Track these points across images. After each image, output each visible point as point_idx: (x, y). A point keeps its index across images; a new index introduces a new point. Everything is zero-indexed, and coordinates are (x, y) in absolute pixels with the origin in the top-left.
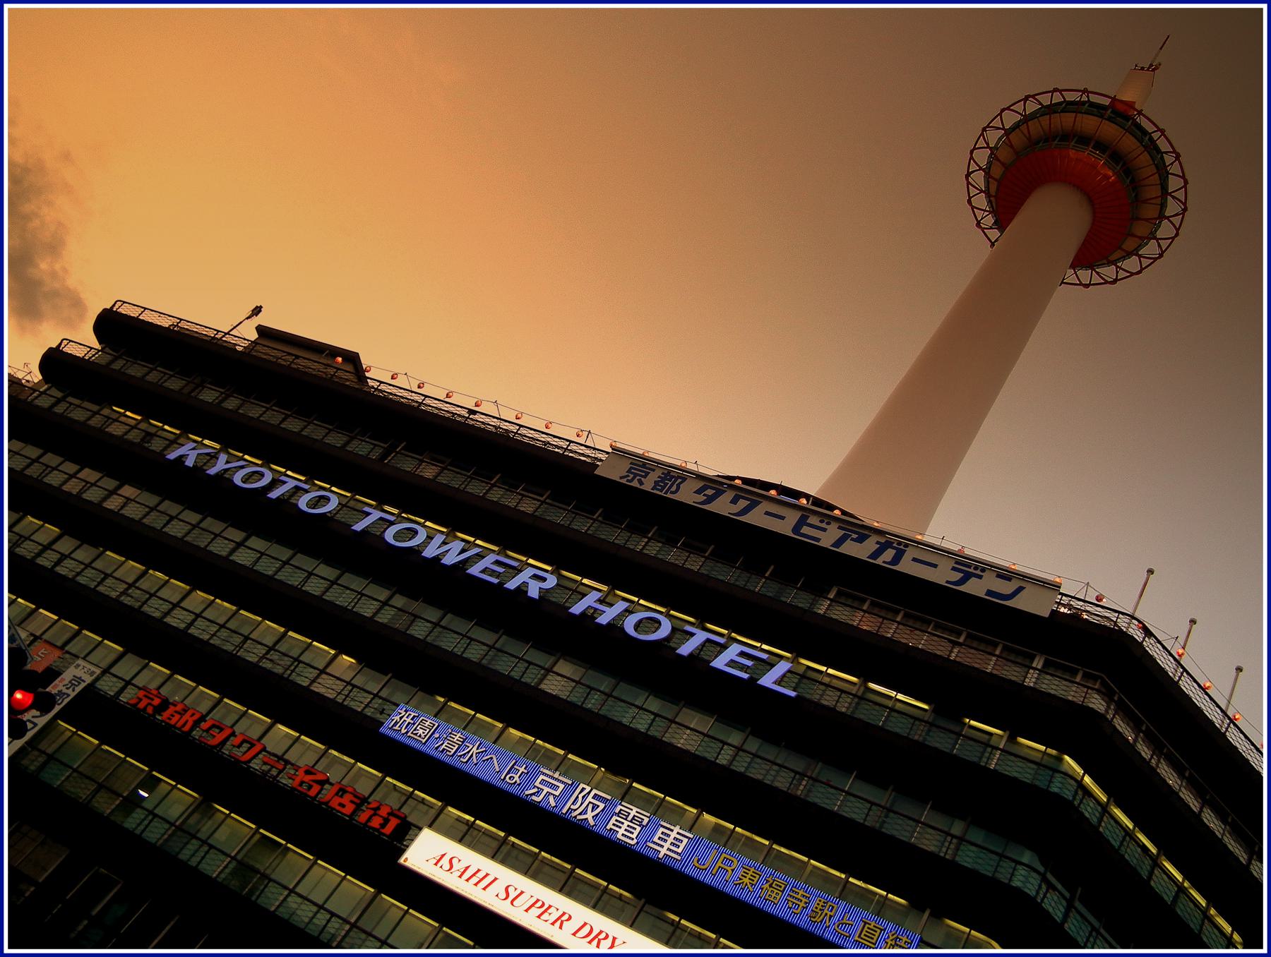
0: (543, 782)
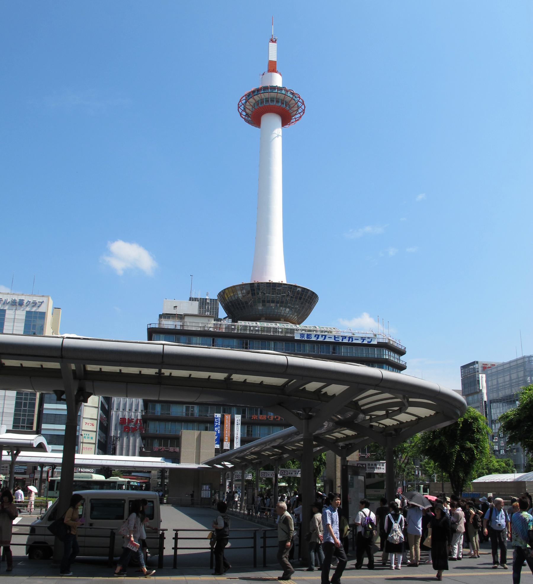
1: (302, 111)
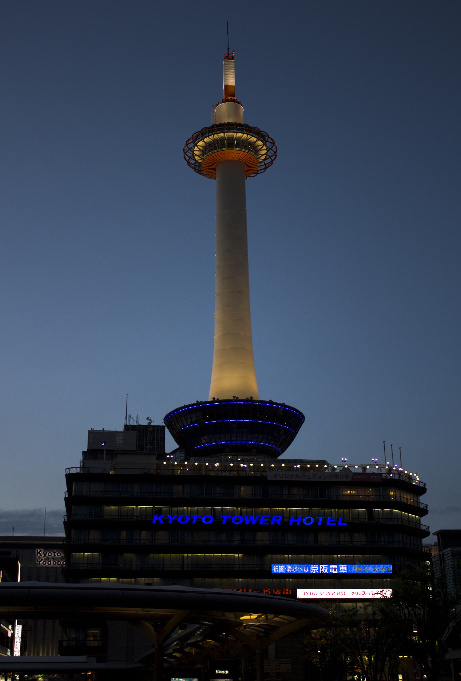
0: (313, 569)
1: (273, 154)
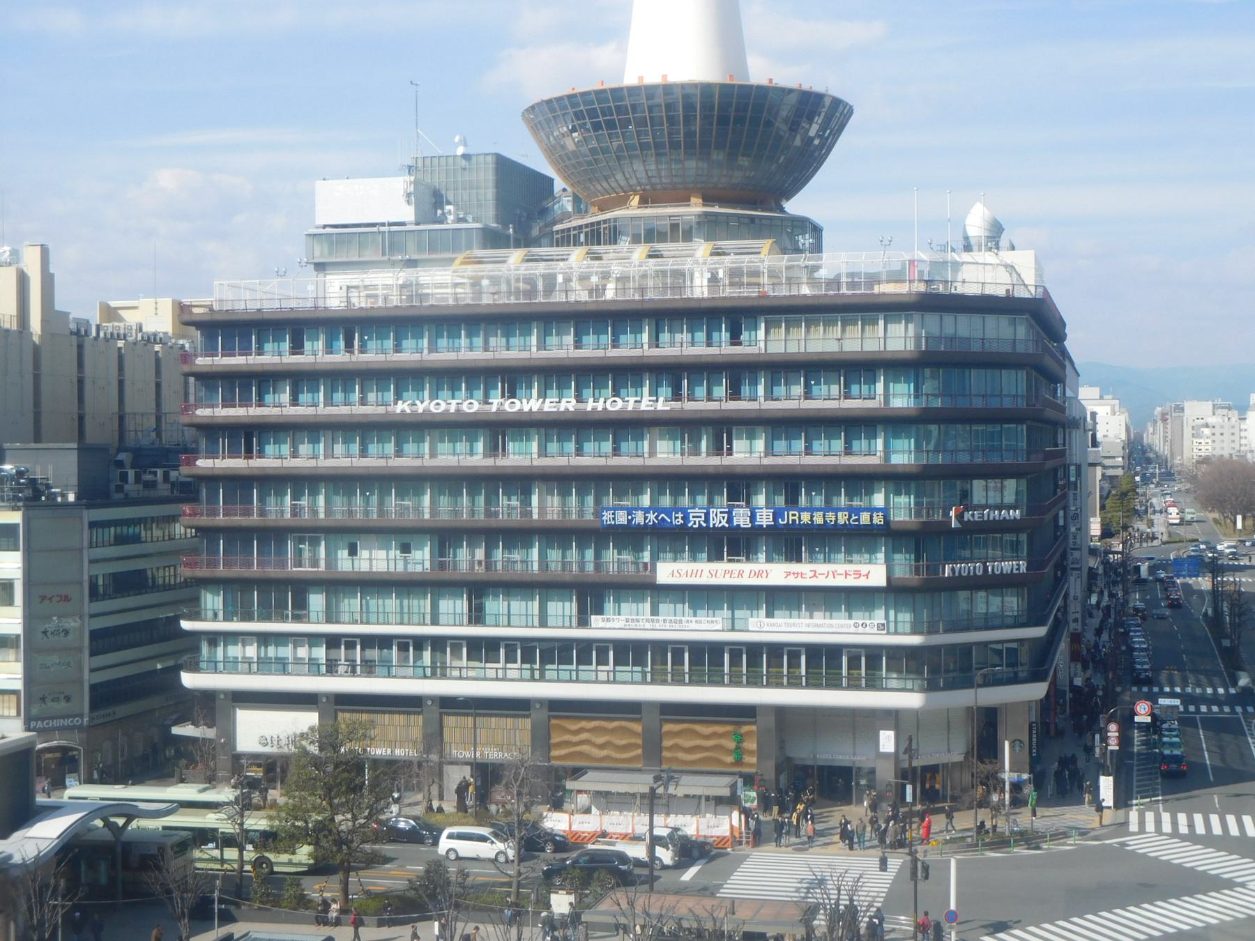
0: (693, 517)
